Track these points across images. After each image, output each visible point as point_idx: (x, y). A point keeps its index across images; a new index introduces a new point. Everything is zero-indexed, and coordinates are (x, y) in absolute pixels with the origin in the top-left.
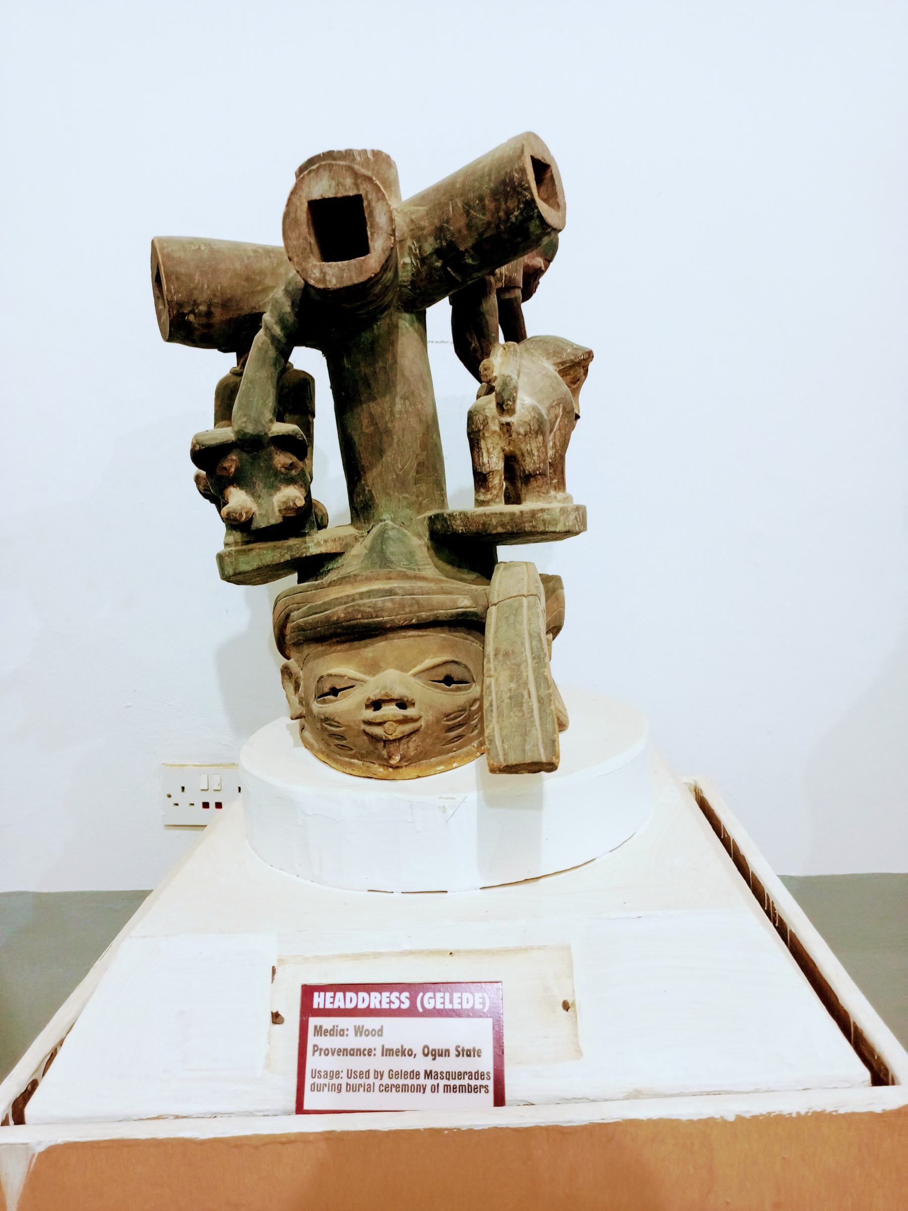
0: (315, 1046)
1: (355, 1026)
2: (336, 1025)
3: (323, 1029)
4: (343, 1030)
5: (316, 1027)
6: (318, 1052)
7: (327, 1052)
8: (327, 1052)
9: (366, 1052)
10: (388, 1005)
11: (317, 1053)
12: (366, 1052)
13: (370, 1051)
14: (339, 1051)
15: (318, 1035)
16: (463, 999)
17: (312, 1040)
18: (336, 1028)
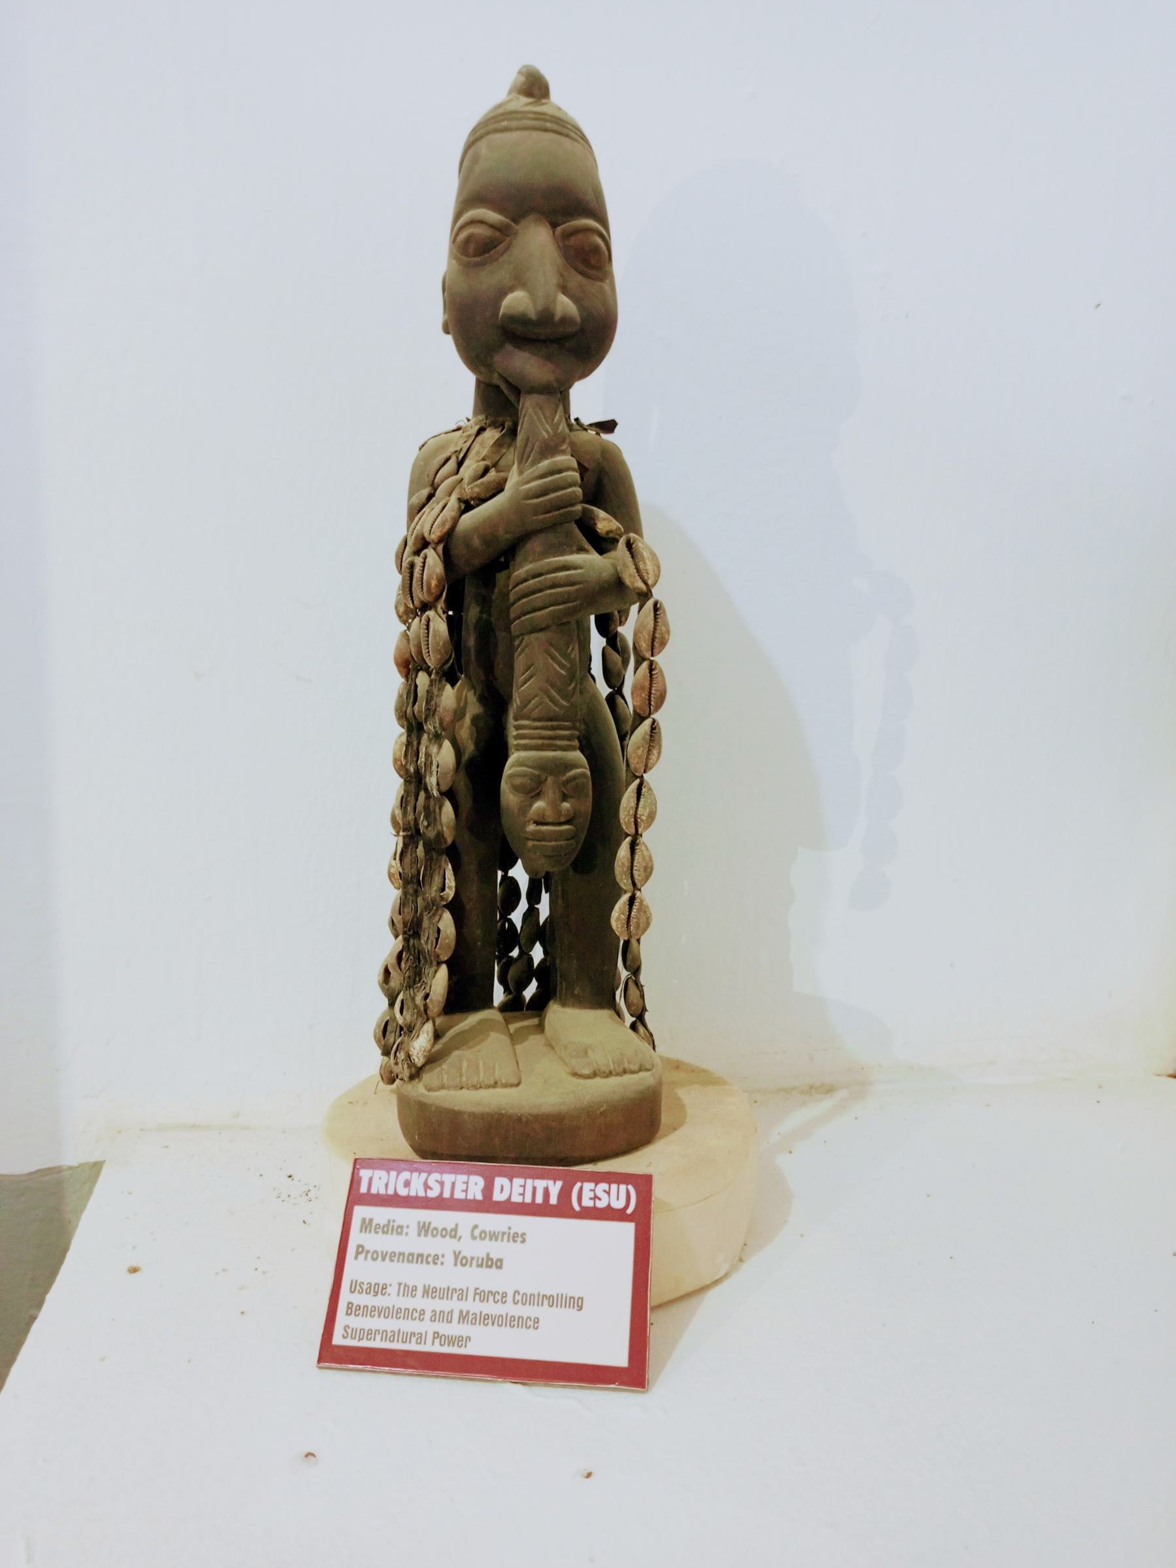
0: (359, 1246)
1: (419, 1223)
2: (392, 1218)
4: (401, 1227)
5: (364, 1220)
7: (375, 1256)
8: (375, 1256)
9: (430, 1259)
10: (592, 1201)
11: (361, 1257)
12: (430, 1259)
13: (436, 1257)
14: (393, 1255)
15: (366, 1231)
16: (469, 1185)
17: (356, 1237)
18: (391, 1224)
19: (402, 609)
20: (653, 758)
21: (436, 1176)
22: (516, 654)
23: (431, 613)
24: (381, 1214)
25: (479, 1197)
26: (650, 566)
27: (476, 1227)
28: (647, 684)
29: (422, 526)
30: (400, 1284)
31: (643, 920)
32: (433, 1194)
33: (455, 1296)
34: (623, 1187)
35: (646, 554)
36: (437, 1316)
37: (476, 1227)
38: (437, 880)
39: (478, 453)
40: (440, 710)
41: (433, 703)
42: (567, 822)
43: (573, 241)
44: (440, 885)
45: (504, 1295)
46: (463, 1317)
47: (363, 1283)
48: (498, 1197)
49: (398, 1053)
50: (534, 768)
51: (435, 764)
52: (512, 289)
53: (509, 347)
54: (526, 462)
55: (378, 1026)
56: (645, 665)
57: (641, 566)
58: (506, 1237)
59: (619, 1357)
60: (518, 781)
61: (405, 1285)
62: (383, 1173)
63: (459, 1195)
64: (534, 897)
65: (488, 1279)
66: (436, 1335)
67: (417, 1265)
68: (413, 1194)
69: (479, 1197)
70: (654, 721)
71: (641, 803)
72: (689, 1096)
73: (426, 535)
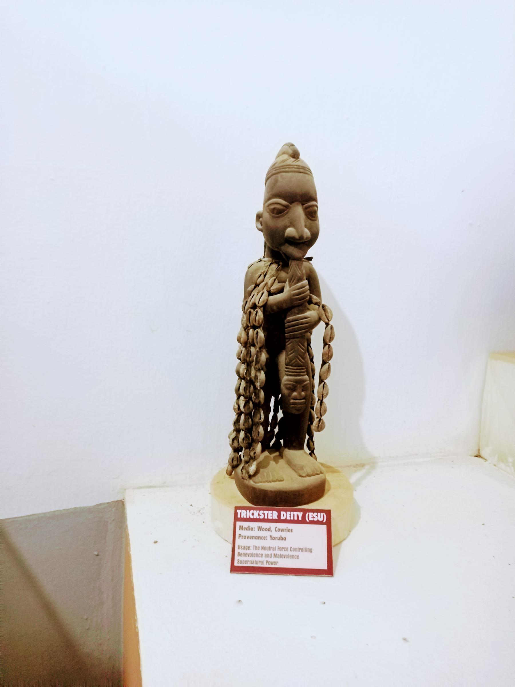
0: (239, 534)
1: (258, 527)
2: (249, 525)
3: (244, 527)
4: (253, 528)
5: (240, 526)
6: (241, 537)
7: (245, 537)
8: (245, 537)
9: (263, 538)
11: (241, 538)
17: (238, 532)
18: (249, 527)
19: (245, 325)
20: (328, 375)
21: (262, 512)
22: (287, 344)
23: (259, 330)
24: (245, 524)
25: (277, 518)
26: (330, 315)
27: (276, 527)
28: (328, 352)
29: (255, 300)
30: (254, 546)
31: (323, 427)
32: (262, 517)
33: (272, 549)
34: (322, 514)
35: (328, 311)
36: (266, 556)
37: (276, 527)
38: (258, 416)
39: (271, 273)
40: (261, 362)
41: (258, 359)
42: (304, 399)
43: (308, 210)
44: (260, 418)
45: (287, 549)
46: (275, 556)
47: (242, 546)
48: (282, 518)
49: (242, 470)
50: (293, 382)
51: (259, 379)
52: (289, 227)
53: (287, 245)
54: (293, 282)
55: (230, 458)
56: (327, 346)
57: (327, 314)
58: (286, 531)
59: (325, 567)
60: (288, 386)
61: (256, 546)
62: (244, 511)
63: (270, 517)
64: (276, 411)
65: (281, 544)
66: (267, 562)
67: (259, 540)
68: (255, 517)
69: (277, 518)
70: (329, 363)
71: (324, 390)
72: (330, 478)
73: (257, 304)
